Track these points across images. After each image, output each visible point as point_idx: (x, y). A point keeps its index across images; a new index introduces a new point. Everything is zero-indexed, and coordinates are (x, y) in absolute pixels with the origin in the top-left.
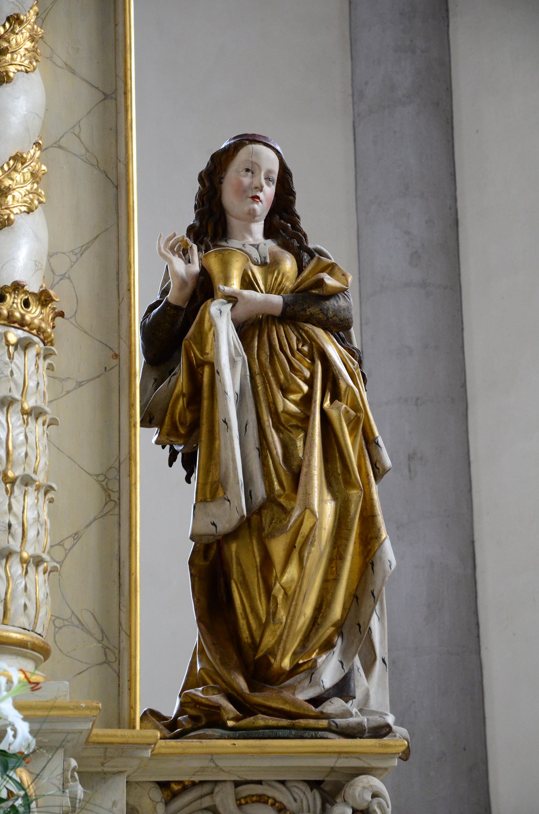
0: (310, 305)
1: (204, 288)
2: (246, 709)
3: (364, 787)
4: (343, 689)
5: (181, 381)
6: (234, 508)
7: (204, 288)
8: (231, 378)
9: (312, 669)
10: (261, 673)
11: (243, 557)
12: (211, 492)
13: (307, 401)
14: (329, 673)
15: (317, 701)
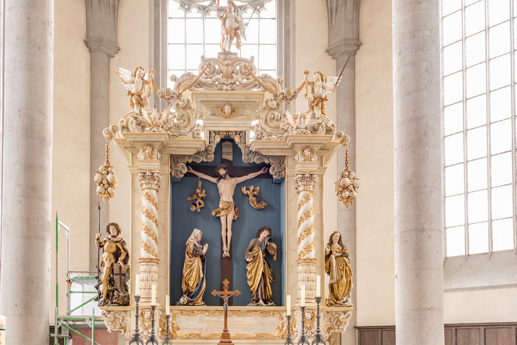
0: (344, 255)
1: (331, 252)
2: (336, 304)
3: (349, 313)
4: (347, 301)
5: (328, 264)
6: (335, 280)
7: (331, 252)
8: (334, 265)
9: (343, 299)
10: (337, 299)
11: (335, 286)
12: (332, 278)
13: (343, 267)
14: (345, 299)
15: (344, 303)
